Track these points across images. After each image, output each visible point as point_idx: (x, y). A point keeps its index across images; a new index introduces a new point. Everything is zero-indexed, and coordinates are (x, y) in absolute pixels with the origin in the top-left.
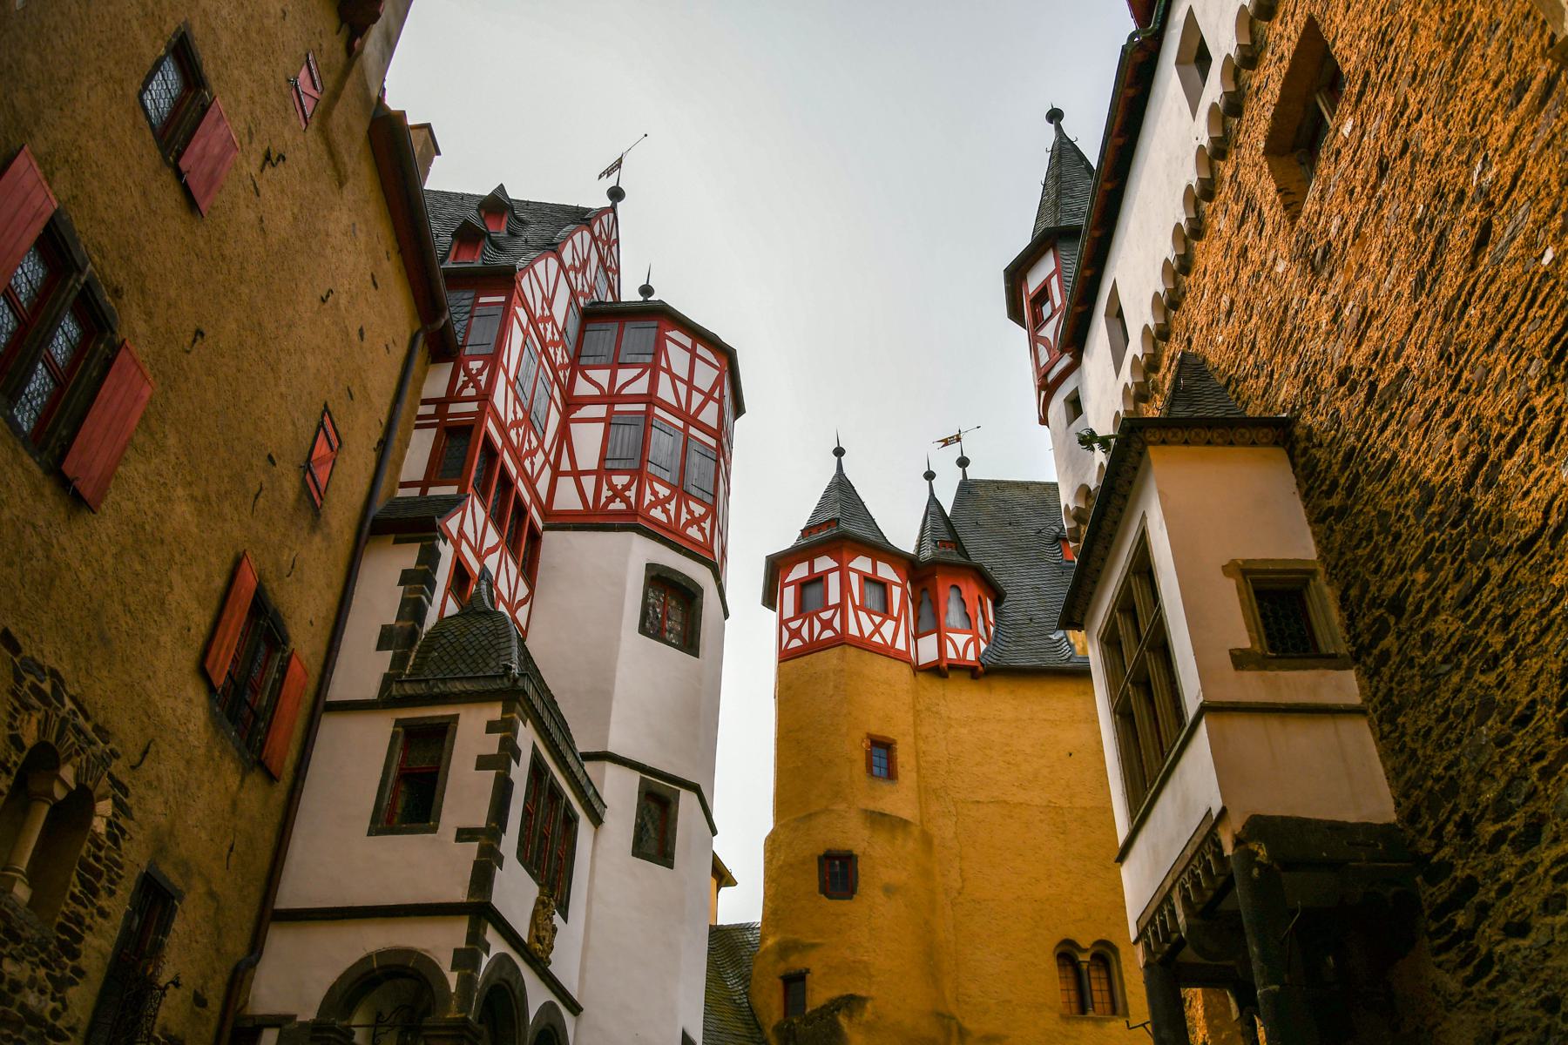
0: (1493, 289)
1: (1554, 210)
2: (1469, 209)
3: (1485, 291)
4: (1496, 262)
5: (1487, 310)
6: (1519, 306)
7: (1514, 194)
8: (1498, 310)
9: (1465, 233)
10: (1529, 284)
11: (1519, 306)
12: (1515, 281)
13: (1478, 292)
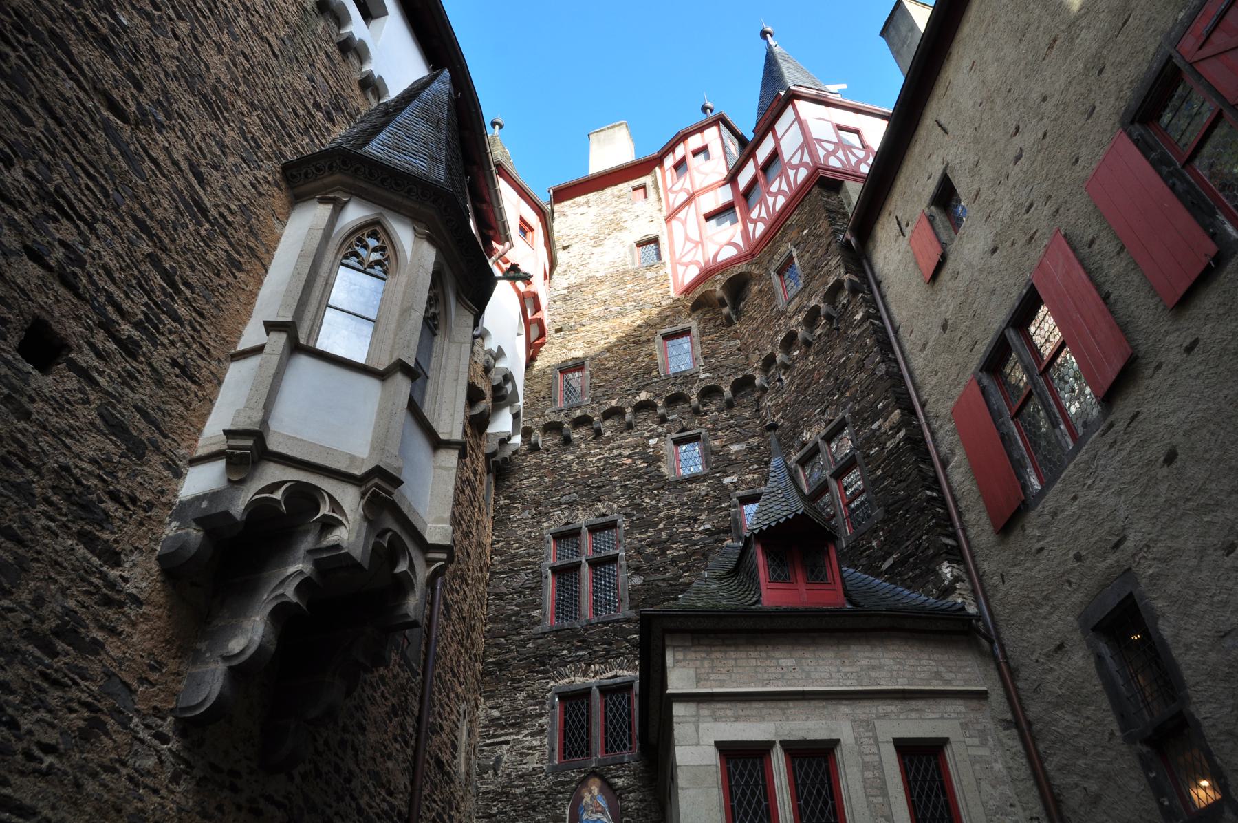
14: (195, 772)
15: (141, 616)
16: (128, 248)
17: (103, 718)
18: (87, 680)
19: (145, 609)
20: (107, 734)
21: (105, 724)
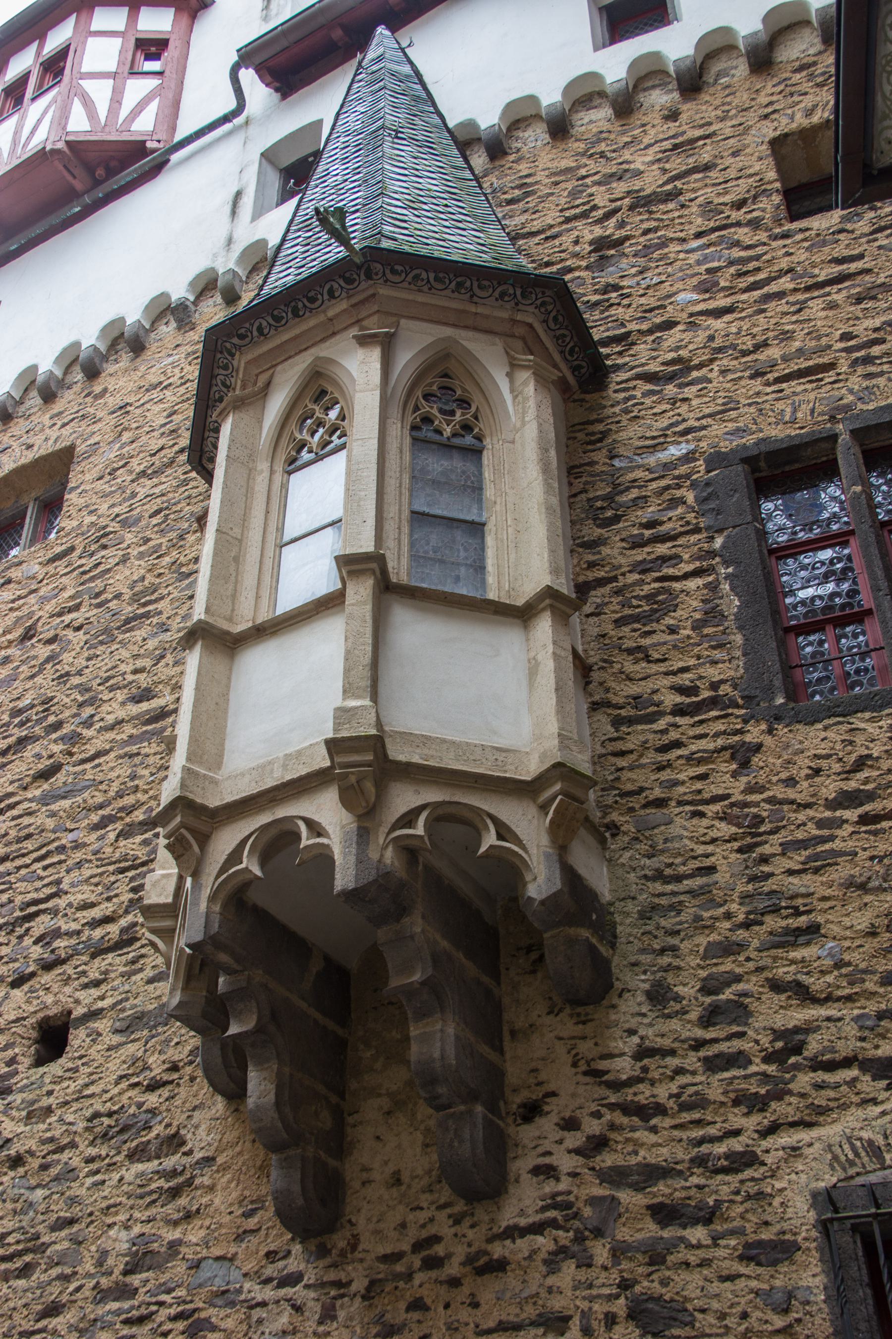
0: (26, 821)
1: (101, 807)
2: (55, 741)
3: (20, 816)
4: (46, 800)
5: (11, 832)
6: (32, 852)
7: (88, 766)
8: (19, 840)
9: (38, 756)
10: (49, 843)
11: (32, 852)
12: (43, 831)
13: (15, 812)
14: (354, 1287)
15: (218, 1171)
16: (97, 860)
17: (203, 1315)
18: (173, 1290)
19: (220, 1160)
20: (214, 1328)
21: (207, 1320)
